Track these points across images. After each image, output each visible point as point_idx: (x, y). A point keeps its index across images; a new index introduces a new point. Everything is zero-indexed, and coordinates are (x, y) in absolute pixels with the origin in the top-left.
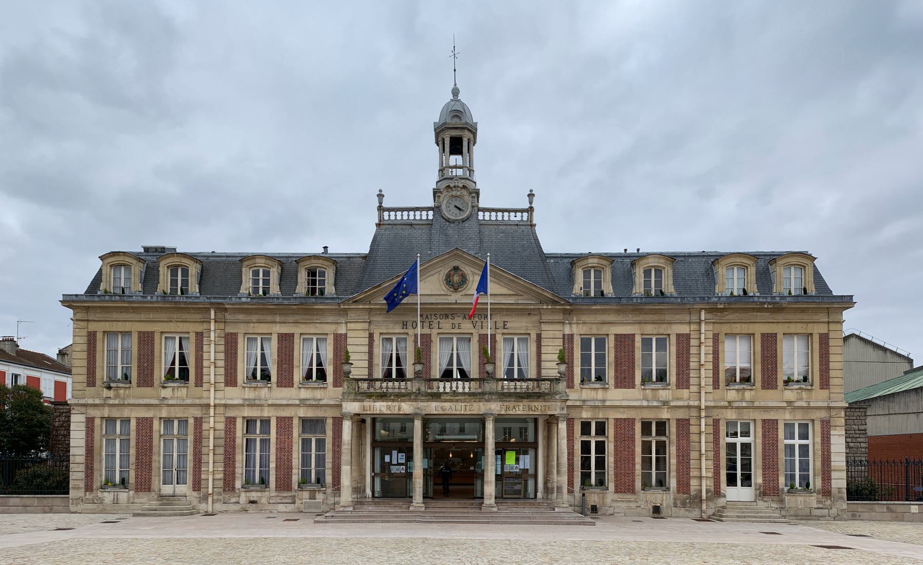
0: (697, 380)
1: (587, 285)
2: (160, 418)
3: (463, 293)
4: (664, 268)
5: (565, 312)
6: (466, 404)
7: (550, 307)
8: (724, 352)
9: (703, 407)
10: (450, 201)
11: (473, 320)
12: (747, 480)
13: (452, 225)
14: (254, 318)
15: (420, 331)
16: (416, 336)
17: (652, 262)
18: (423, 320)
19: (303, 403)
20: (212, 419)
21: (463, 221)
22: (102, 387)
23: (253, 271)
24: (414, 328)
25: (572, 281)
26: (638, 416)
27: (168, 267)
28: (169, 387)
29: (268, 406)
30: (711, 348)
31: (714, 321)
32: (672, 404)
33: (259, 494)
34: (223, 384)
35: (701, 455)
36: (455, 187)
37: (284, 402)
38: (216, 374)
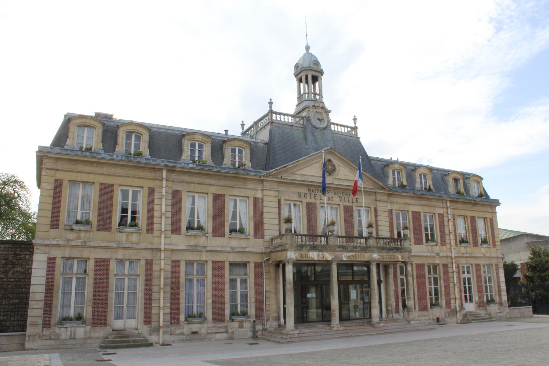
0: (449, 240)
3: (334, 177)
5: (389, 195)
6: (360, 254)
7: (382, 192)
8: (457, 225)
9: (453, 257)
10: (315, 115)
12: (471, 300)
13: (317, 130)
14: (195, 179)
18: (311, 193)
19: (233, 250)
21: (324, 129)
24: (306, 198)
26: (426, 262)
28: (125, 232)
29: (206, 252)
32: (441, 255)
33: (199, 326)
34: (170, 232)
35: (454, 285)
36: (317, 106)
37: (219, 249)
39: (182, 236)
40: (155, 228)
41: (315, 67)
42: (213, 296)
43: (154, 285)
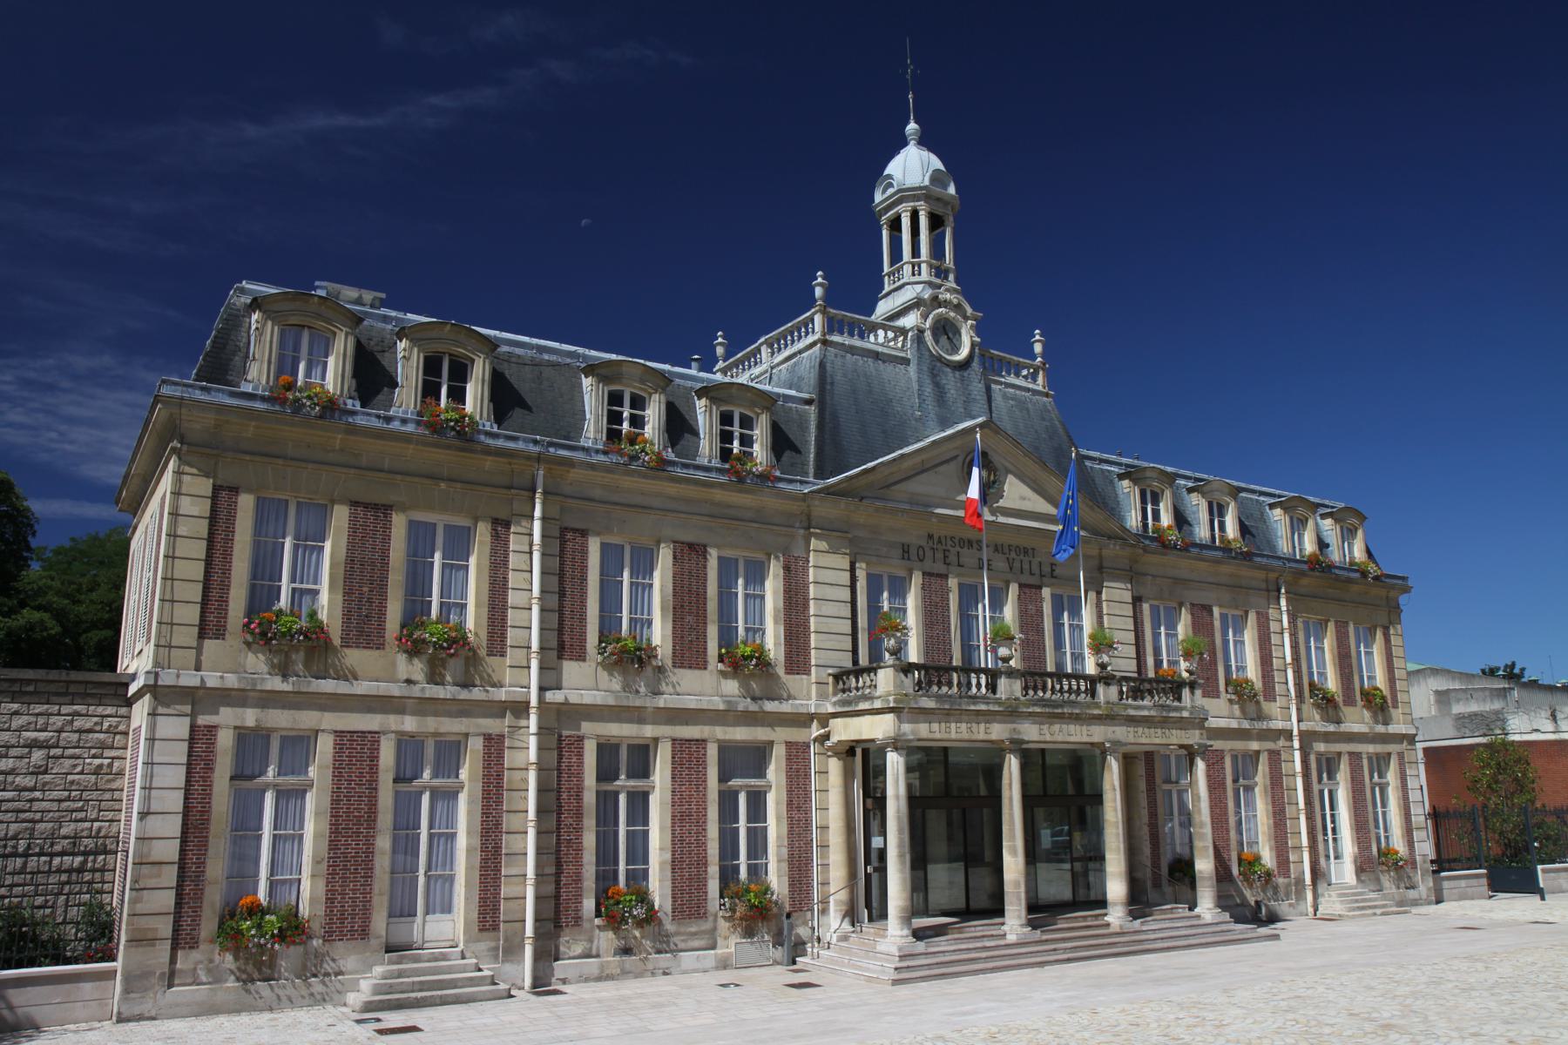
9: (1295, 732)
34: (554, 654)
39: (587, 664)
42: (674, 844)
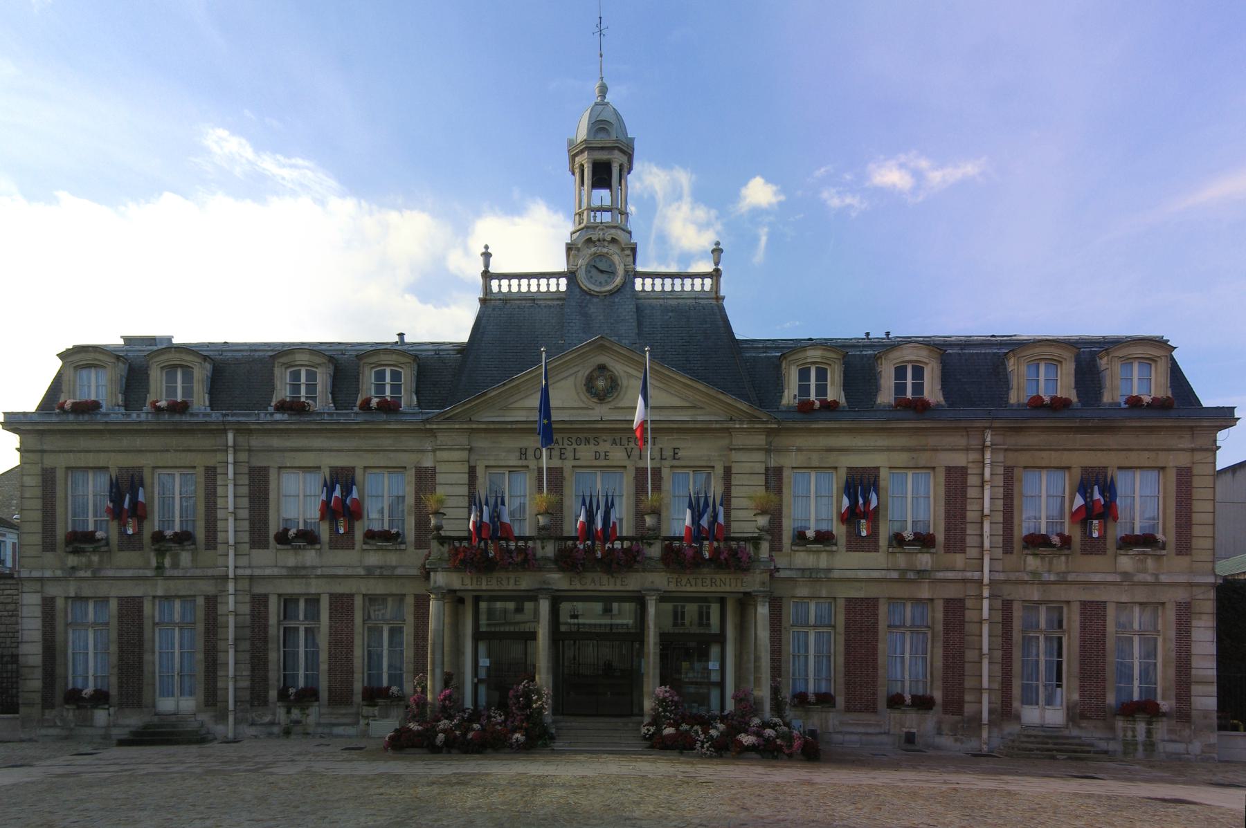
1: (804, 390)
2: (154, 597)
3: (612, 405)
4: (926, 364)
5: (770, 432)
7: (745, 426)
11: (626, 446)
13: (595, 300)
15: (547, 463)
16: (540, 470)
17: (908, 354)
19: (370, 573)
20: (231, 599)
21: (612, 293)
22: (67, 552)
23: (290, 372)
25: (781, 385)
27: (162, 368)
29: (315, 578)
30: (1001, 490)
31: (1006, 447)
34: (247, 546)
36: (599, 240)
37: (340, 572)
38: (238, 529)
40: (219, 541)
41: (603, 139)
43: (220, 640)
